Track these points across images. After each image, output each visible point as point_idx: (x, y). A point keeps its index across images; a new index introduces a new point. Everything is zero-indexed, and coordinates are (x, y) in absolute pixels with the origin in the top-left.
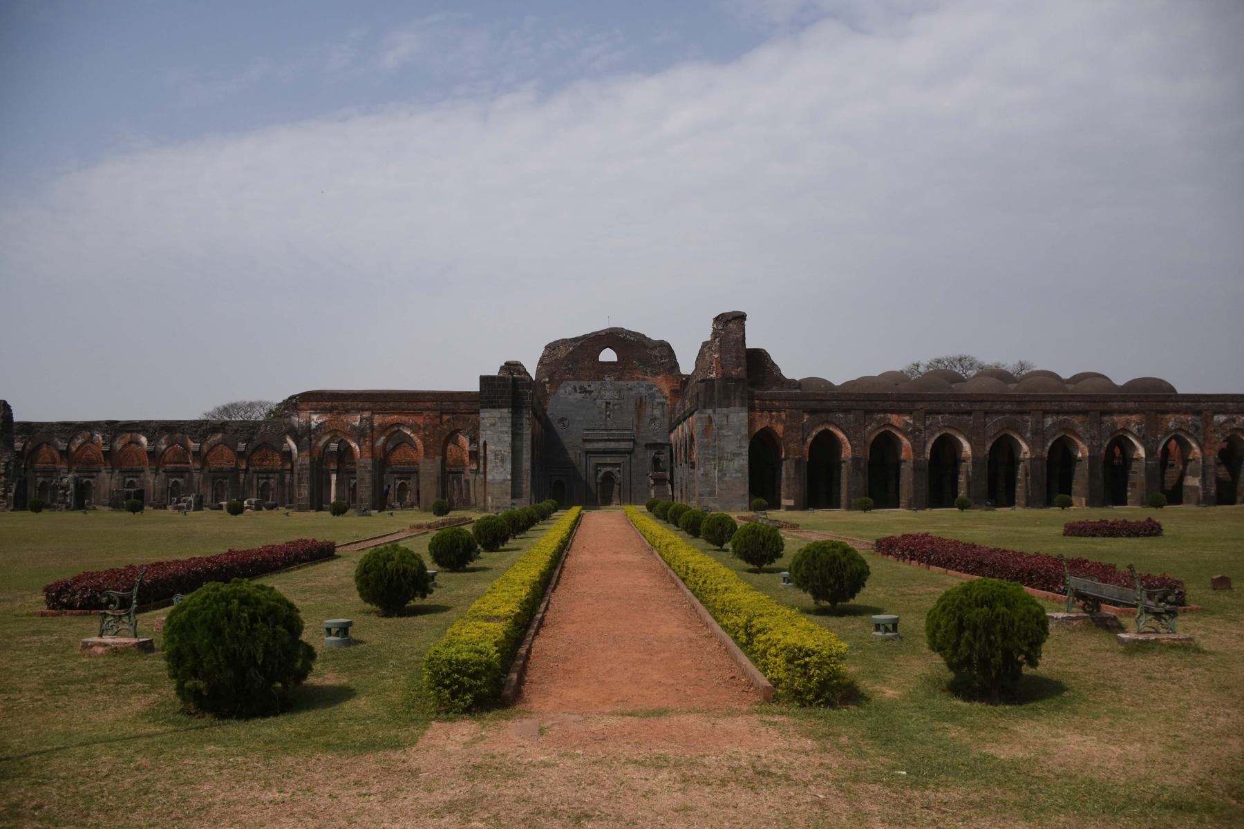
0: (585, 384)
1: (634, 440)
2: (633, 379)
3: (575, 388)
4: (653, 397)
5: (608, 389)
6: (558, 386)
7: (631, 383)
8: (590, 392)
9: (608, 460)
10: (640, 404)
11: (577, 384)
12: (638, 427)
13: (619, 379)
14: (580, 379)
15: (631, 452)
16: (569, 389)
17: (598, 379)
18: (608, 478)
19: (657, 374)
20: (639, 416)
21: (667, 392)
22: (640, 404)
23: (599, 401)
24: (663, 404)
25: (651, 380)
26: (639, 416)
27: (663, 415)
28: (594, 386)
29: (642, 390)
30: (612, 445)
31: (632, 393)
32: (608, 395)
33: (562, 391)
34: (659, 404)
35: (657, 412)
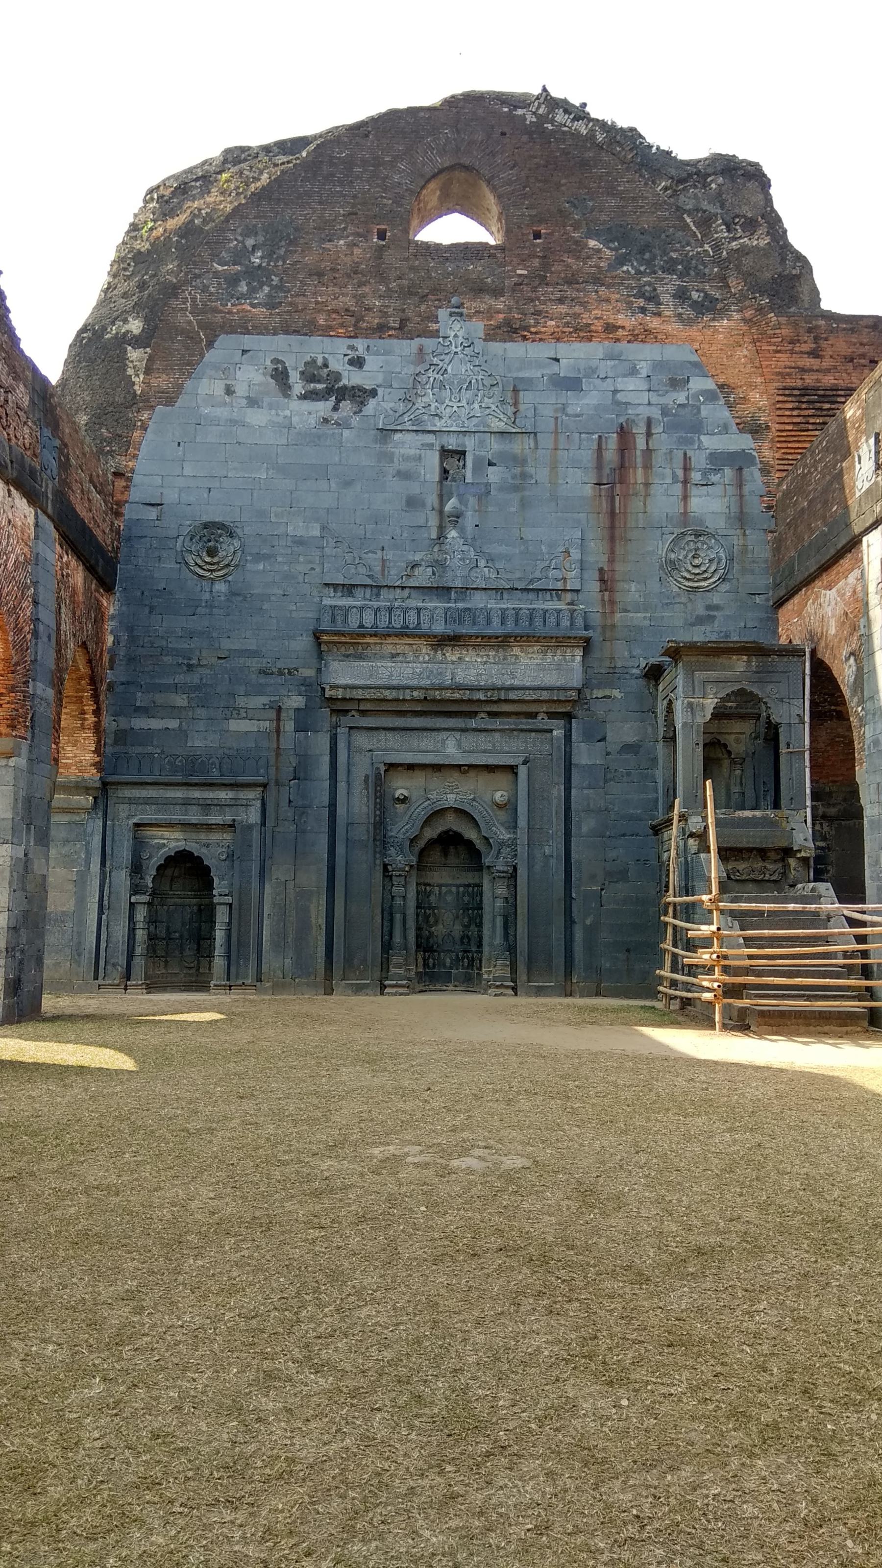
0: (333, 352)
1: (587, 645)
2: (584, 333)
3: (280, 375)
4: (688, 425)
5: (453, 381)
6: (189, 365)
7: (575, 354)
8: (360, 396)
9: (451, 748)
10: (620, 466)
11: (295, 351)
12: (606, 582)
13: (511, 330)
14: (310, 329)
15: (566, 708)
16: (251, 376)
17: (403, 330)
18: (452, 844)
19: (708, 307)
20: (614, 527)
21: (759, 400)
22: (620, 466)
23: (406, 444)
24: (738, 461)
25: (678, 340)
26: (614, 527)
27: (741, 519)
28: (383, 363)
29: (633, 389)
30: (472, 669)
31: (583, 404)
32: (461, 410)
33: (206, 387)
34: (719, 460)
35: (710, 505)
